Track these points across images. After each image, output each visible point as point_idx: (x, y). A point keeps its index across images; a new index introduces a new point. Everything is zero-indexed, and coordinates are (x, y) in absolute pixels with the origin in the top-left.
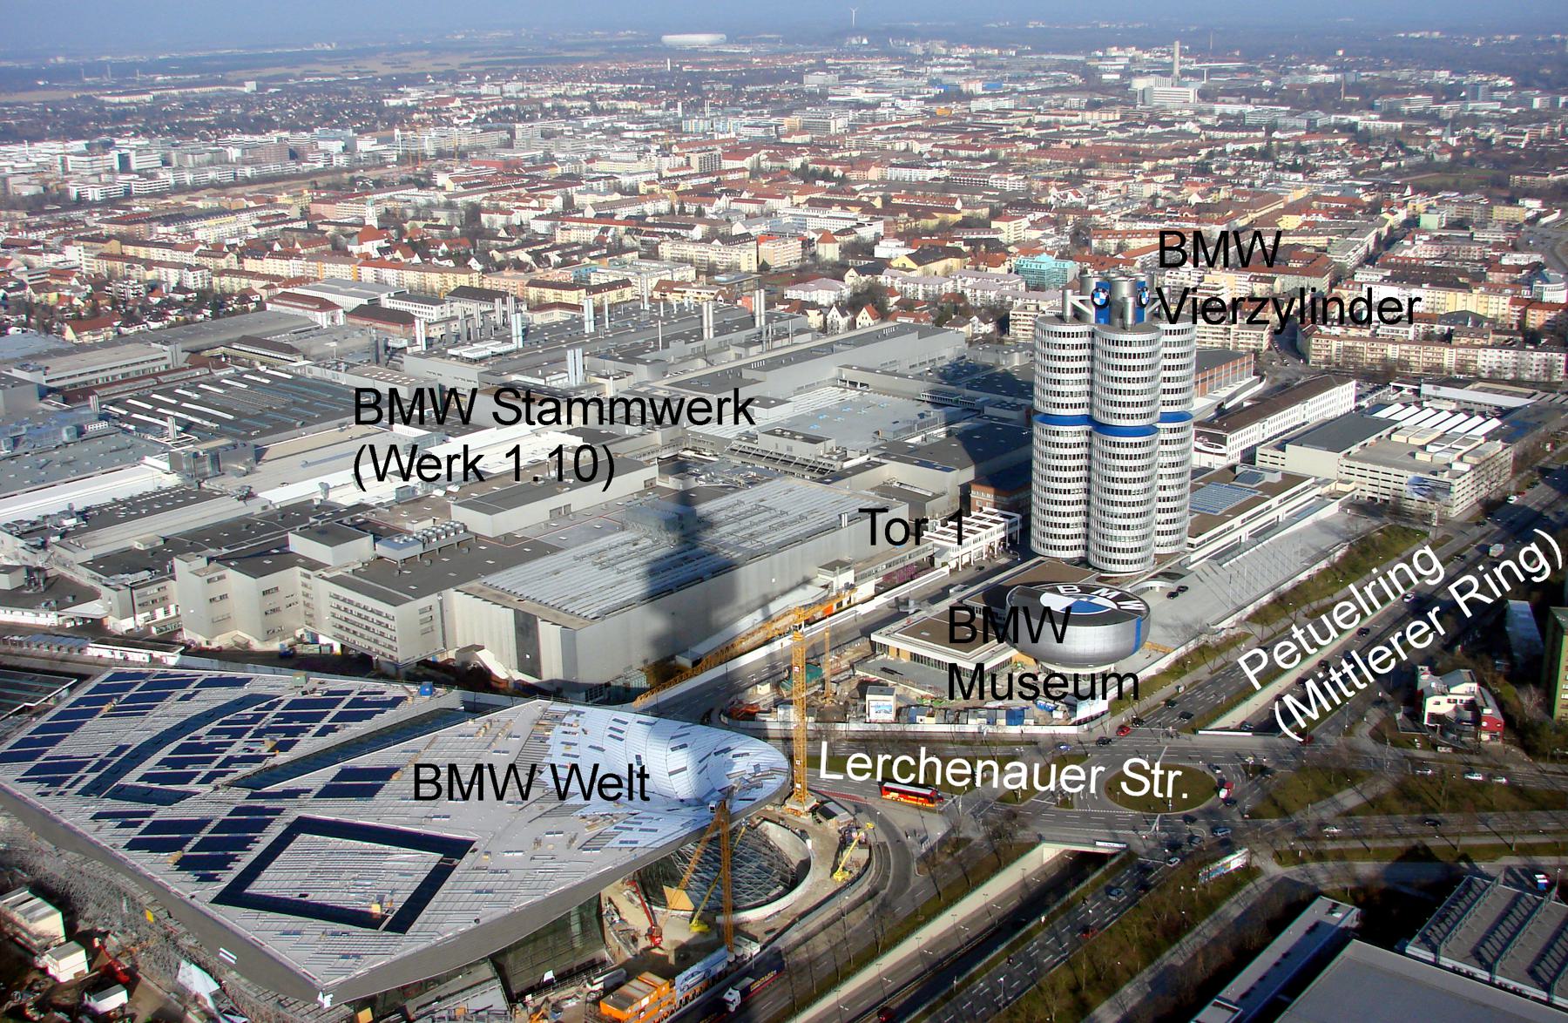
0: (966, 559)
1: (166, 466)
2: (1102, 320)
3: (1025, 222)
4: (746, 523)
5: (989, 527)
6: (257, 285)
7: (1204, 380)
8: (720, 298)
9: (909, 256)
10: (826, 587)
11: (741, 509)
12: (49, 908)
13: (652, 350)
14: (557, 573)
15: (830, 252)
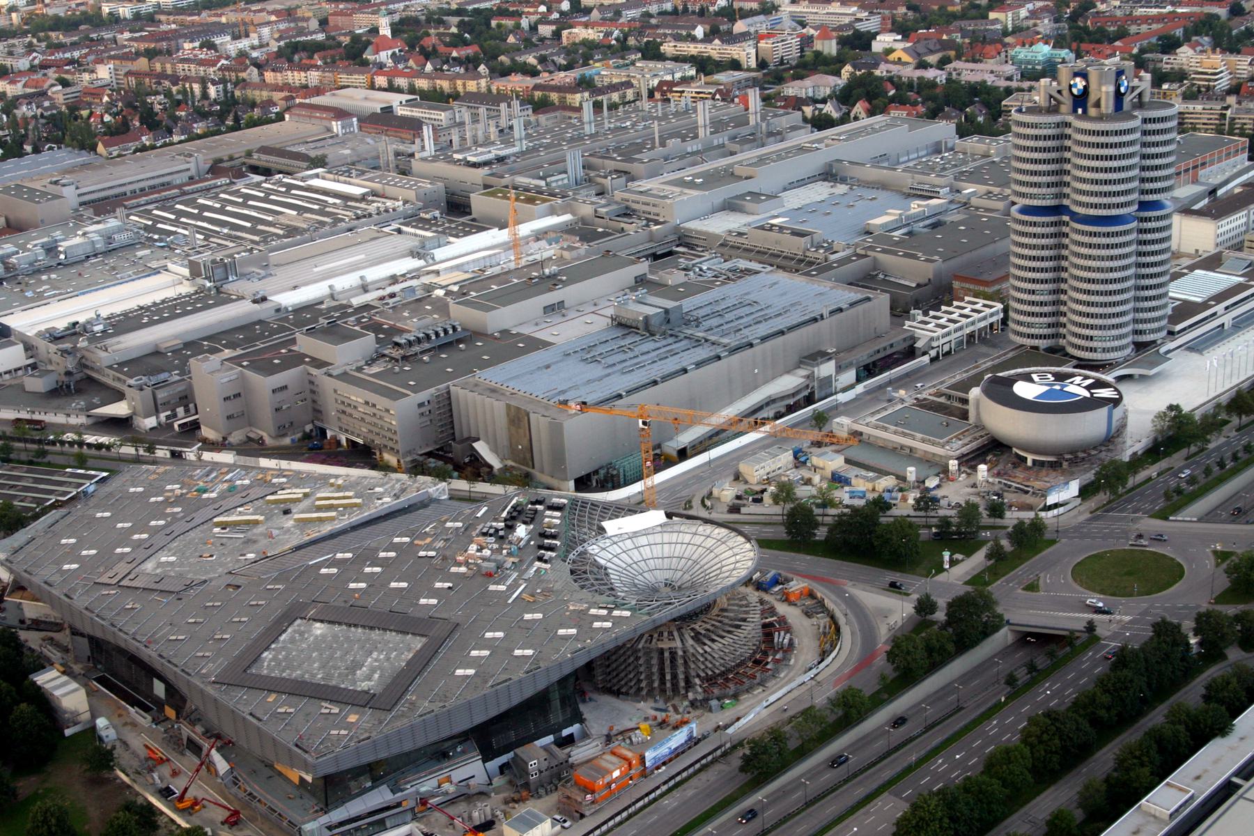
0: (946, 348)
1: (186, 272)
2: (1080, 111)
3: (1023, 13)
4: (729, 317)
5: (967, 317)
6: (277, 96)
7: (1195, 167)
8: (718, 96)
9: (904, 50)
10: (808, 377)
11: (728, 303)
12: (74, 685)
13: (649, 149)
14: (548, 367)
15: (830, 48)
